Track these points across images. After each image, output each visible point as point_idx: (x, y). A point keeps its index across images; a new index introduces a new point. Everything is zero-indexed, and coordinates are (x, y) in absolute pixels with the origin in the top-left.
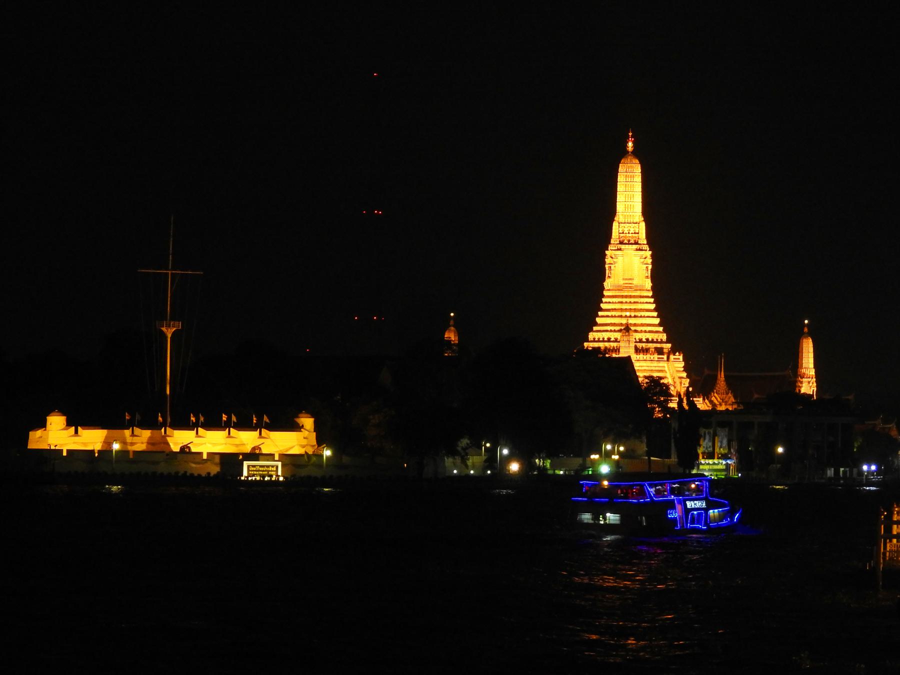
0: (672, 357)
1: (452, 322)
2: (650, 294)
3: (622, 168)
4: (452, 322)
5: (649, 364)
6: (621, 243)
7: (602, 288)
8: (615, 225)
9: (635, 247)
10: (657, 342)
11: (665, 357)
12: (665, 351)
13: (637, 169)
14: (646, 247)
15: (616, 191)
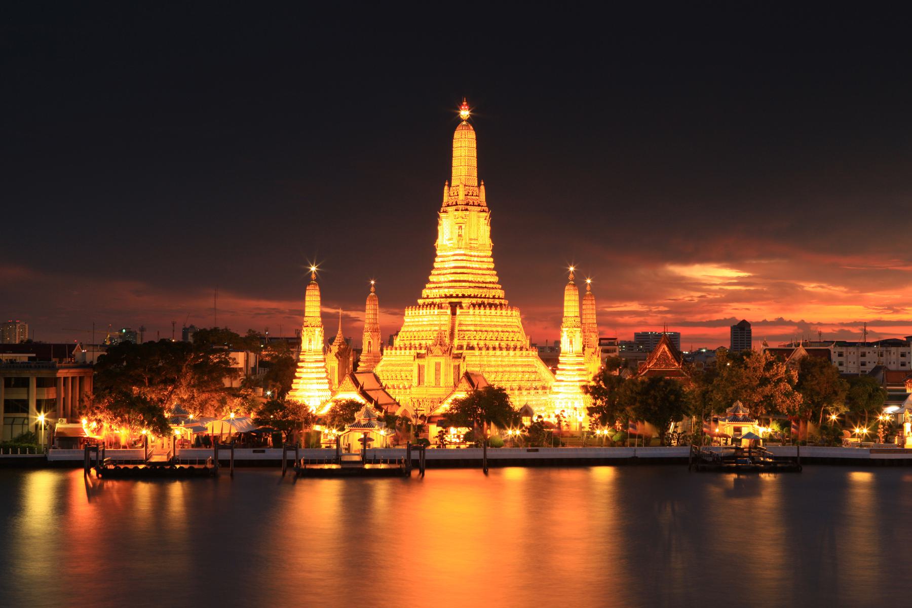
0: (458, 311)
1: (372, 289)
2: (490, 253)
3: (457, 135)
4: (372, 289)
5: (431, 318)
6: (448, 206)
7: (434, 249)
8: (446, 188)
9: (454, 208)
10: (457, 296)
11: (449, 311)
12: (464, 305)
13: (472, 135)
14: (486, 209)
15: (452, 156)
